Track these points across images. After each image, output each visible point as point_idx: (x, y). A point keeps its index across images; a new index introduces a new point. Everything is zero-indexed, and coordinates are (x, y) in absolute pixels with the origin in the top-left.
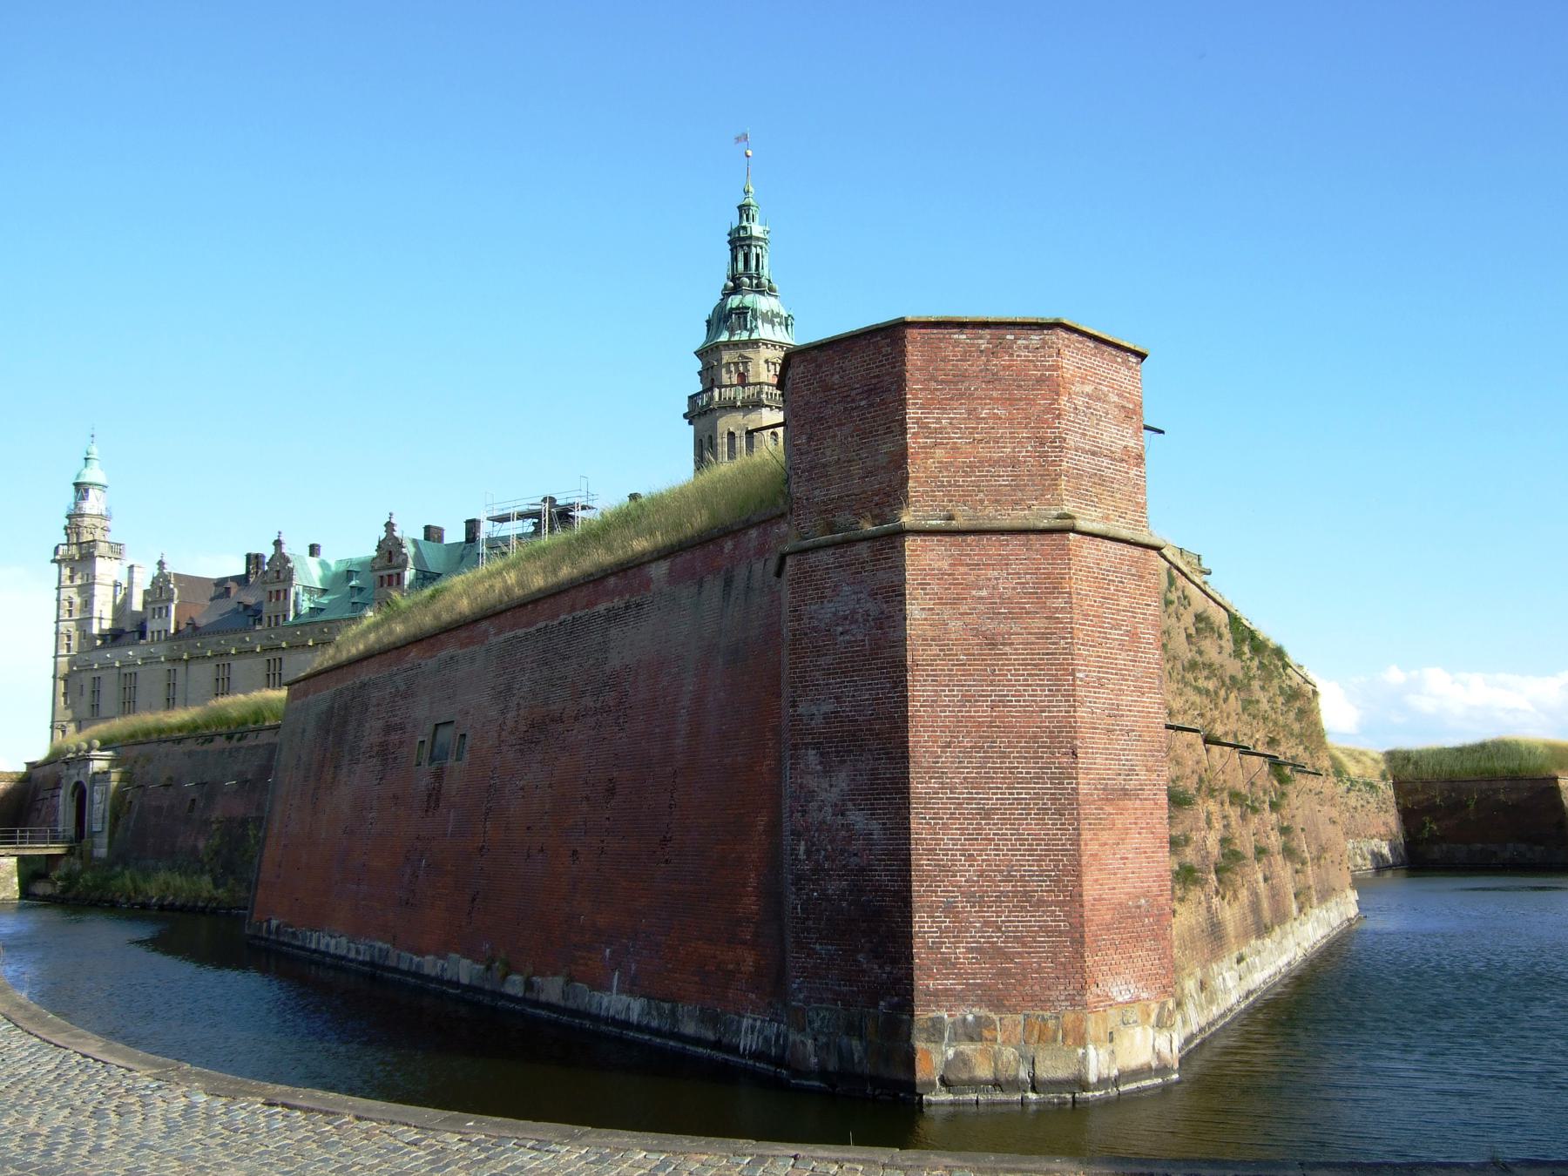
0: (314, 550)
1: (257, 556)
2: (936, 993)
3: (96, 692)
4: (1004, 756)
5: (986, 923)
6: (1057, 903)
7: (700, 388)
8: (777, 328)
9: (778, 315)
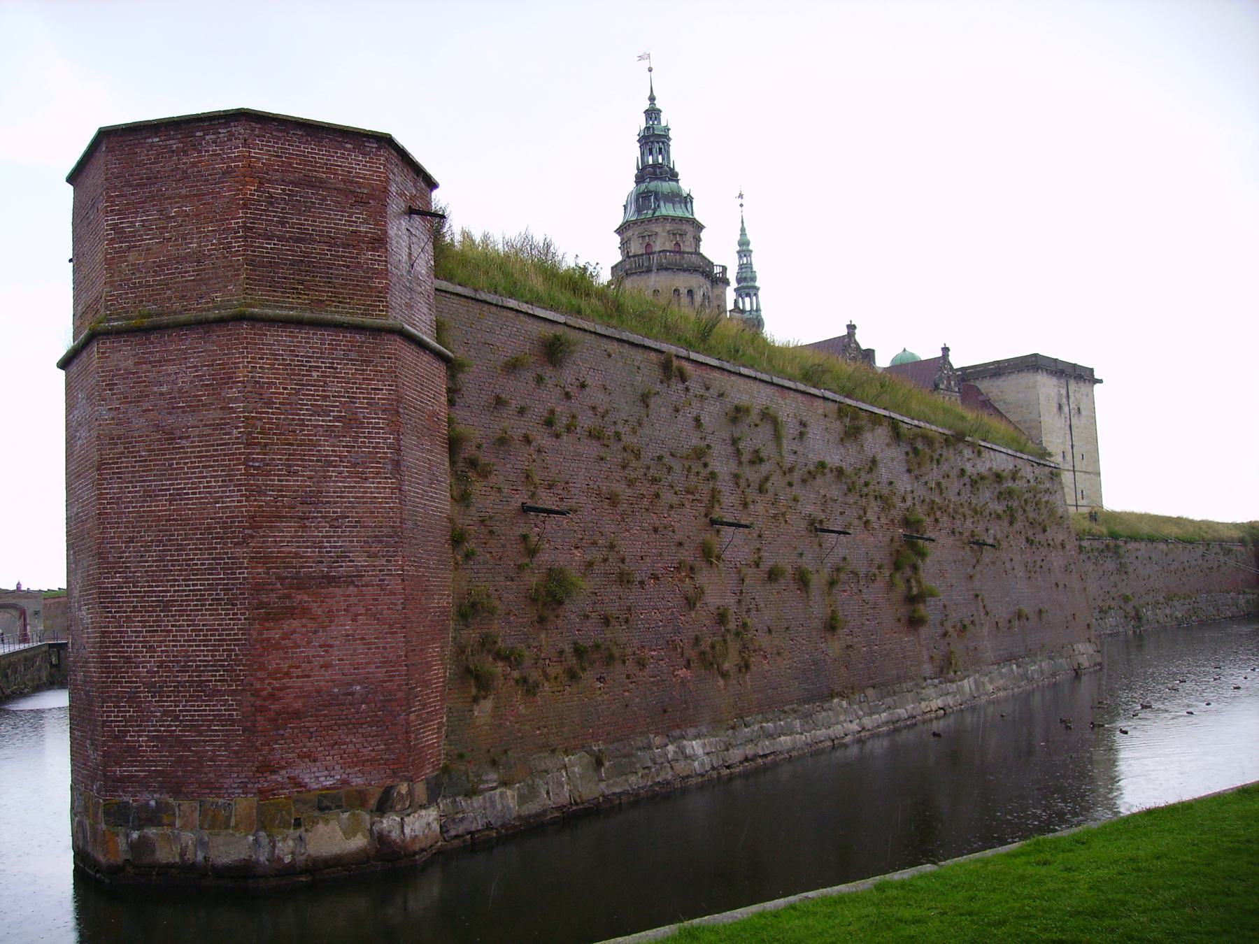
2: (122, 779)
4: (181, 548)
5: (165, 713)
6: (231, 693)
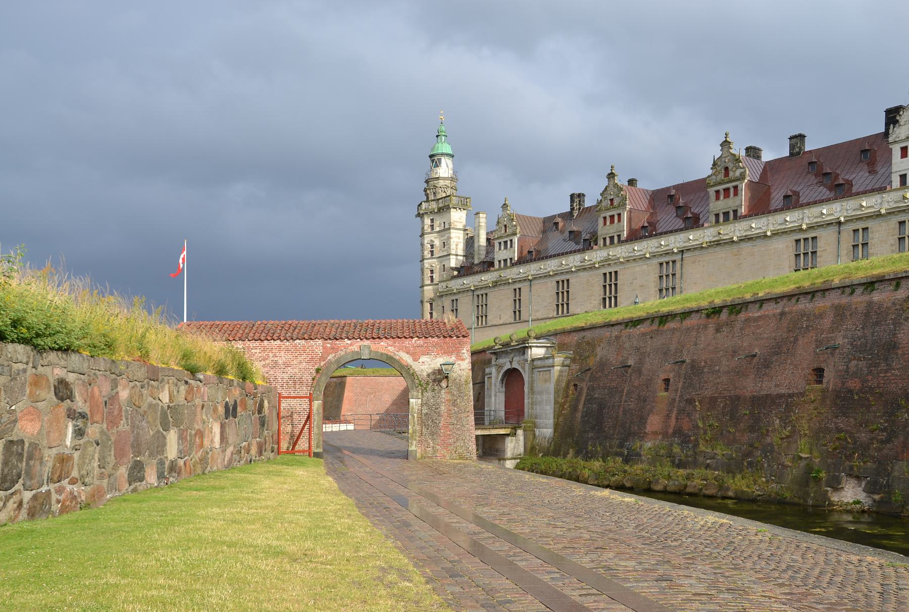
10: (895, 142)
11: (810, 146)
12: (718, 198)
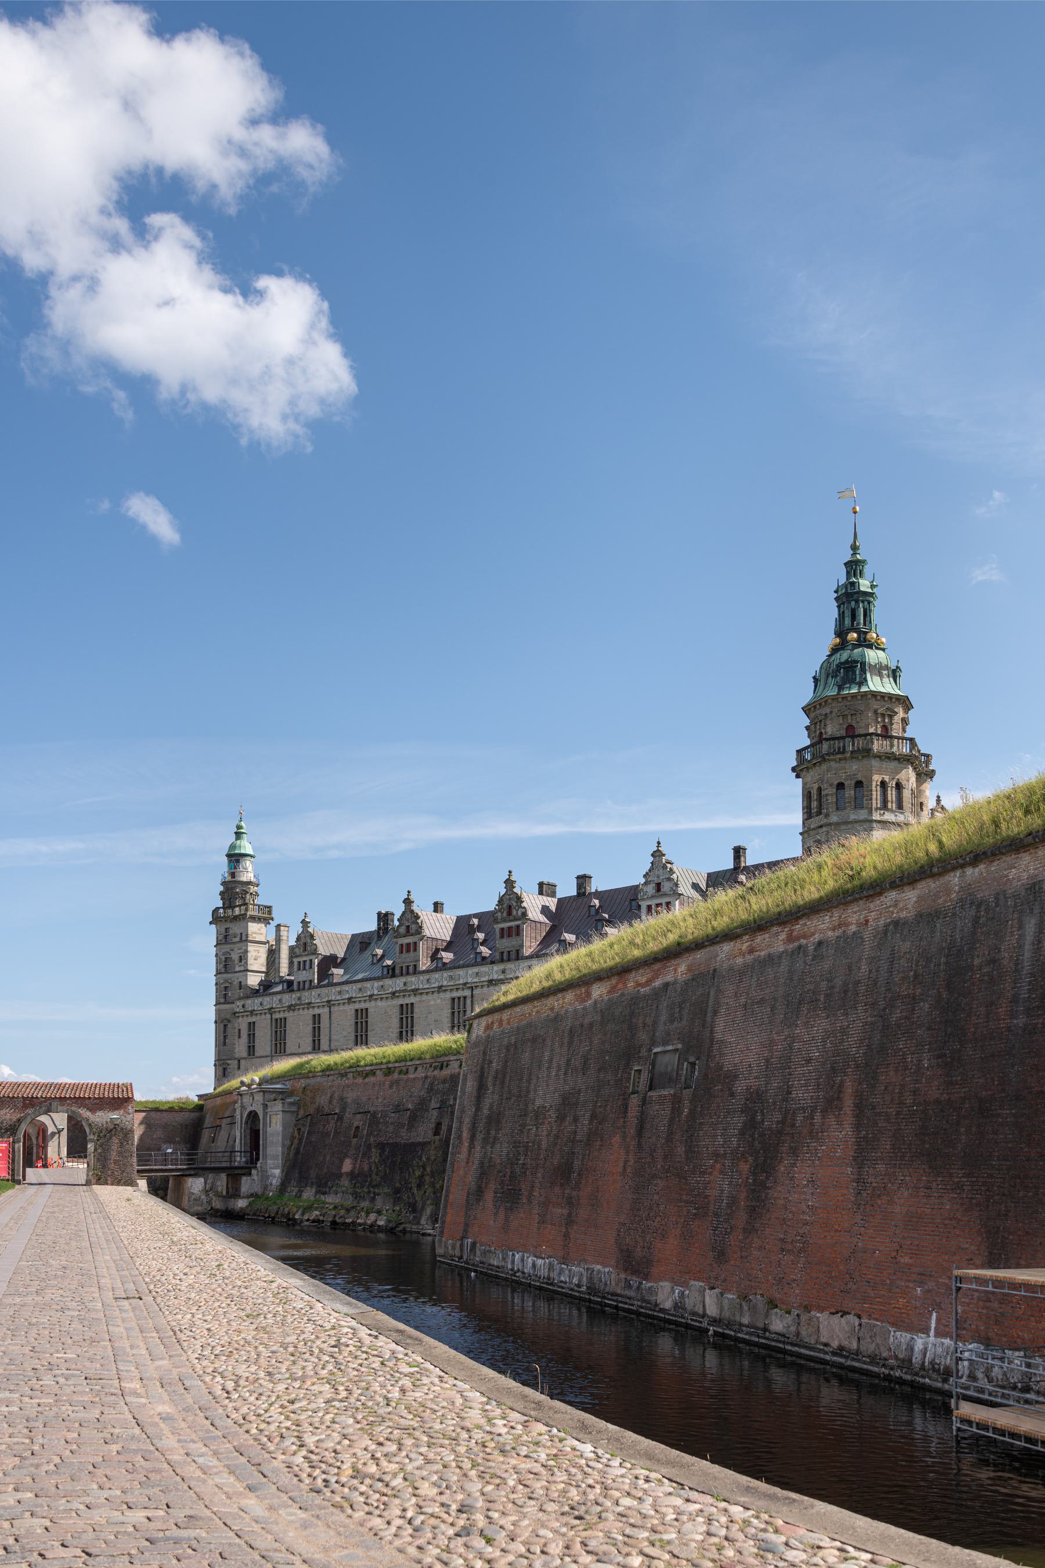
0: (437, 907)
1: (387, 914)
3: (252, 1037)
7: (807, 742)
8: (886, 680)
9: (887, 668)
10: (643, 899)
11: (595, 886)
12: (502, 937)
